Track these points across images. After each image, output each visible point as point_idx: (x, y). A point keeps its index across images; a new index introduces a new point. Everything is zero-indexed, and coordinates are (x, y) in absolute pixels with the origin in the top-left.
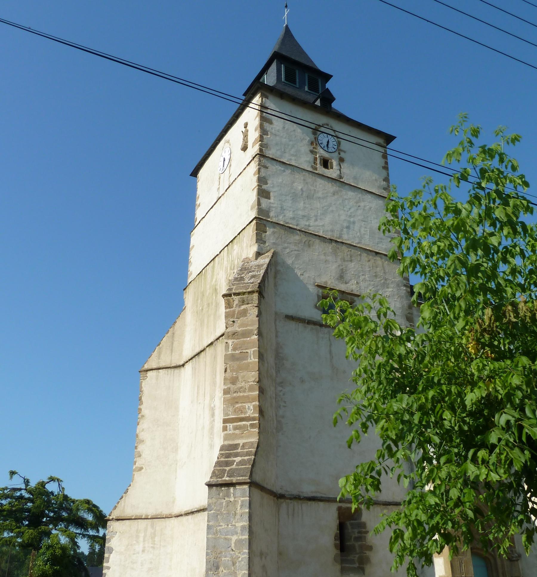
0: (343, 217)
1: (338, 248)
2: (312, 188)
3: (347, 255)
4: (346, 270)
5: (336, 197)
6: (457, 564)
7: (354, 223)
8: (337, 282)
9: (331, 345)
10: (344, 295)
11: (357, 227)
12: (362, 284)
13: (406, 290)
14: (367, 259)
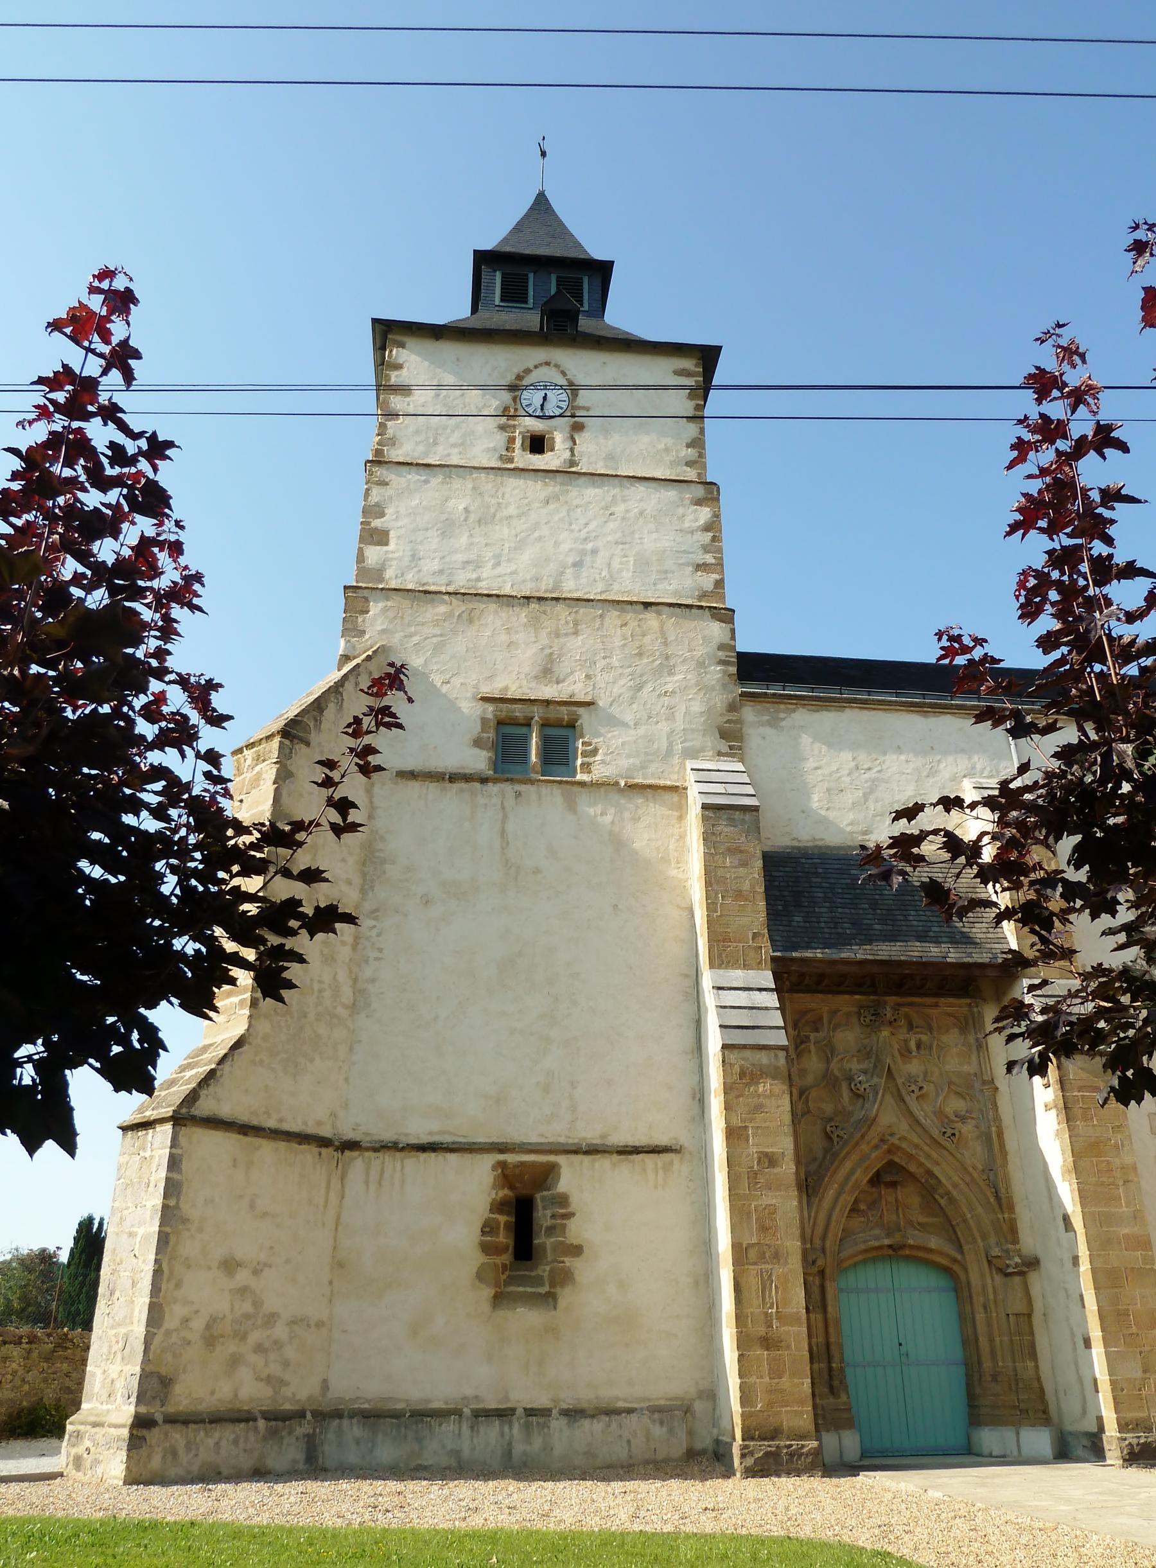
0: (565, 547)
1: (545, 612)
2: (494, 501)
3: (567, 623)
4: (560, 656)
5: (552, 506)
6: (753, 1281)
7: (595, 552)
8: (533, 685)
9: (505, 818)
10: (551, 707)
11: (600, 560)
12: (601, 679)
13: (725, 672)
14: (619, 623)
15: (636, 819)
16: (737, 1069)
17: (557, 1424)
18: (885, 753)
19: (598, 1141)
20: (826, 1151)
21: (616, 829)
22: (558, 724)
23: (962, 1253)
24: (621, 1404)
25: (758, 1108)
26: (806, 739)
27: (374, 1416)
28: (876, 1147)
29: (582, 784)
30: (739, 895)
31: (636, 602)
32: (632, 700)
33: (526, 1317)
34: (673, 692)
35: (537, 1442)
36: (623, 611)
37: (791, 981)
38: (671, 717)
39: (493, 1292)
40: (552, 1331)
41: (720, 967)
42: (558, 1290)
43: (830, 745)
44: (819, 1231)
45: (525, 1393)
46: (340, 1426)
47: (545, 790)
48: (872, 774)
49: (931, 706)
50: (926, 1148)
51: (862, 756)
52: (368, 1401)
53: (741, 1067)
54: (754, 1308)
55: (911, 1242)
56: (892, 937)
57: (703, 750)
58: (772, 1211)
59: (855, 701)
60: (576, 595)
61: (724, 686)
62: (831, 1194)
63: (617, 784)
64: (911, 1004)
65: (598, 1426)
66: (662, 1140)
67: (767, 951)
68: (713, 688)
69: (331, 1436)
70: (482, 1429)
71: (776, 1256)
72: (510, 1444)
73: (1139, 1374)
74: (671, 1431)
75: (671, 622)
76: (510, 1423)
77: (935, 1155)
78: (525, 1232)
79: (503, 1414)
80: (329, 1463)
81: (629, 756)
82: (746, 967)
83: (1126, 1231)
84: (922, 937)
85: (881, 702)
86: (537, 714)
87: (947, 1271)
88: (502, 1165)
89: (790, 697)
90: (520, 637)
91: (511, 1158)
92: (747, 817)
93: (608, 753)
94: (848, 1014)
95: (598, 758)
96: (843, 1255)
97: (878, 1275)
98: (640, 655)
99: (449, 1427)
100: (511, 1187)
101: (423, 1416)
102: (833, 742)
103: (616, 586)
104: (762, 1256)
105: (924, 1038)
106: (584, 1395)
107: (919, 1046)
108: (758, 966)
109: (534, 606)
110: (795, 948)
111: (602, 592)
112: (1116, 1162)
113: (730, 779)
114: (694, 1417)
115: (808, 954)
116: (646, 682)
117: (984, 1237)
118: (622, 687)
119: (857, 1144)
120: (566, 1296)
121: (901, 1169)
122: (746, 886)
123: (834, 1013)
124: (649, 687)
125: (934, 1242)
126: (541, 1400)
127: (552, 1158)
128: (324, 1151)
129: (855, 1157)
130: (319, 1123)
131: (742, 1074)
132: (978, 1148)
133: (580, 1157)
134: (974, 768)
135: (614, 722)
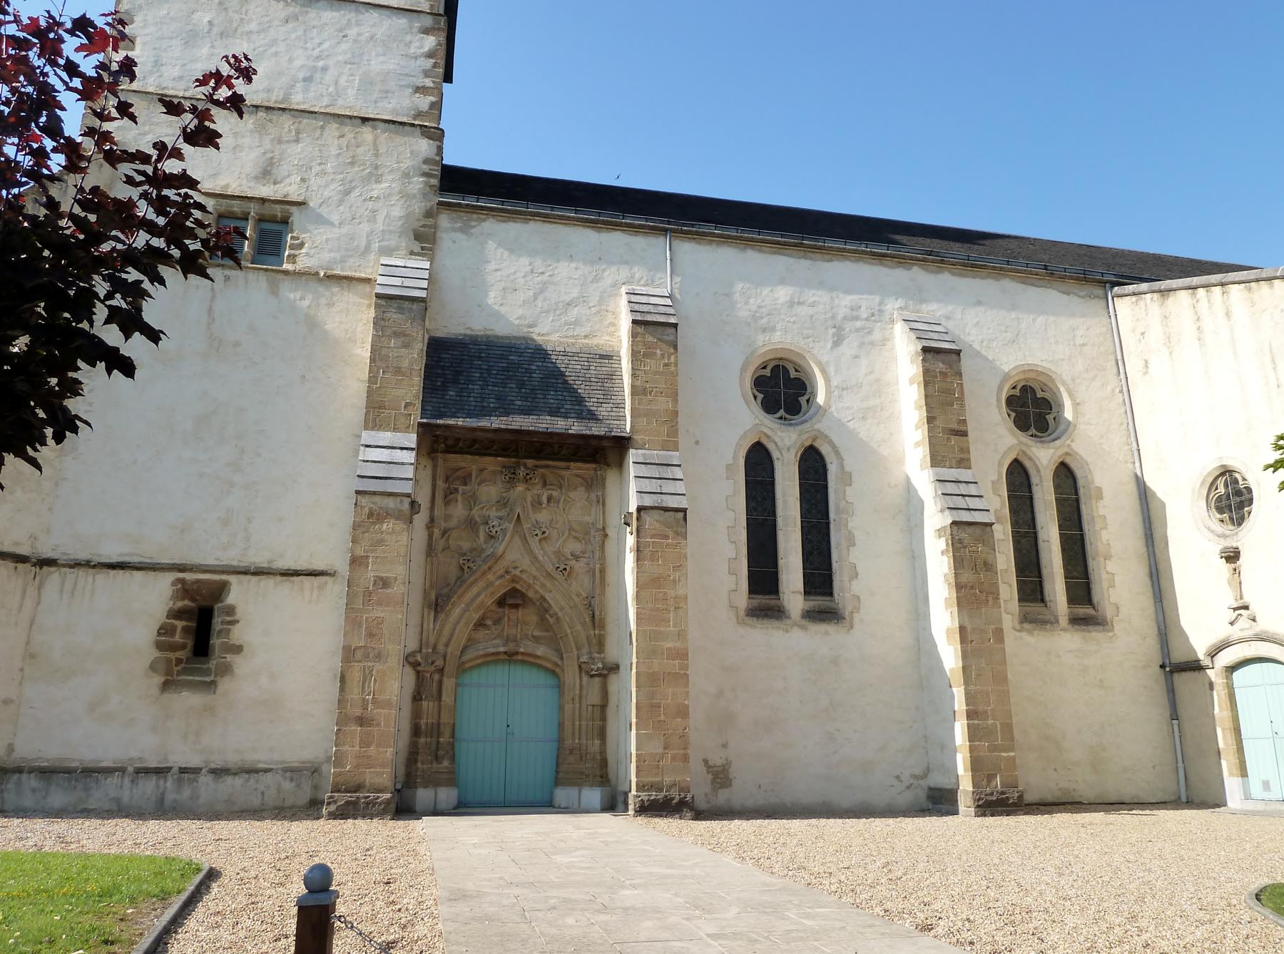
0: (298, 63)
1: (270, 121)
2: (237, 17)
3: (290, 131)
4: (280, 160)
5: (290, 25)
7: (325, 69)
8: (252, 184)
9: (213, 297)
10: (267, 204)
11: (329, 78)
12: (314, 182)
13: (426, 183)
14: (337, 134)
15: (331, 305)
16: (366, 510)
17: (205, 780)
18: (558, 261)
19: (265, 565)
20: (458, 578)
21: (312, 312)
22: (273, 220)
23: (562, 658)
24: (261, 766)
25: (381, 542)
26: (491, 245)
27: (48, 773)
28: (502, 576)
29: (286, 272)
30: (398, 371)
31: (355, 117)
32: (341, 202)
33: (189, 700)
34: (378, 198)
35: (187, 792)
36: (342, 124)
37: (435, 442)
38: (372, 219)
39: (163, 679)
40: (210, 710)
41: (372, 429)
42: (218, 679)
43: (511, 251)
44: (443, 640)
45: (182, 755)
46: (19, 779)
47: (252, 276)
48: (545, 278)
49: (604, 222)
50: (542, 579)
51: (538, 263)
52: (48, 761)
53: (371, 510)
54: (354, 694)
55: (522, 650)
56: (527, 412)
57: (397, 249)
58: (380, 622)
59: (538, 215)
60: (302, 107)
61: (424, 195)
62: (457, 612)
63: (317, 274)
64: (547, 467)
65: (238, 781)
66: (319, 565)
67: (416, 417)
68: (414, 196)
69: (11, 786)
70: (141, 782)
71: (379, 656)
72: (163, 794)
73: (660, 750)
74: (298, 786)
75: (385, 137)
76: (165, 778)
77: (548, 584)
78: (198, 633)
79: (160, 772)
80: (7, 806)
81: (331, 251)
82: (395, 430)
83: (670, 645)
84: (554, 412)
85: (561, 217)
86: (253, 210)
87: (553, 672)
88: (182, 581)
89: (482, 208)
90: (247, 141)
91: (188, 576)
92: (415, 306)
93: (313, 247)
94: (494, 473)
95: (303, 251)
96: (464, 658)
97: (499, 674)
98: (352, 164)
99: (114, 780)
100: (193, 599)
101: (91, 773)
102: (513, 248)
103: (340, 102)
104: (366, 656)
105: (555, 494)
106: (232, 759)
107: (549, 500)
108: (406, 429)
109: (261, 114)
110: (441, 416)
111: (327, 106)
112: (672, 593)
113: (408, 272)
114: (320, 775)
115: (451, 422)
116: (354, 188)
117: (578, 649)
118: (332, 191)
119: (484, 573)
120: (225, 685)
121: (523, 596)
122: (405, 364)
123: (482, 470)
124: (357, 192)
125: (541, 650)
126: (194, 761)
127: (224, 577)
128: (20, 566)
129: (481, 584)
130: (17, 544)
131: (370, 515)
132: (586, 580)
133: (249, 577)
134: (633, 277)
135: (321, 220)
